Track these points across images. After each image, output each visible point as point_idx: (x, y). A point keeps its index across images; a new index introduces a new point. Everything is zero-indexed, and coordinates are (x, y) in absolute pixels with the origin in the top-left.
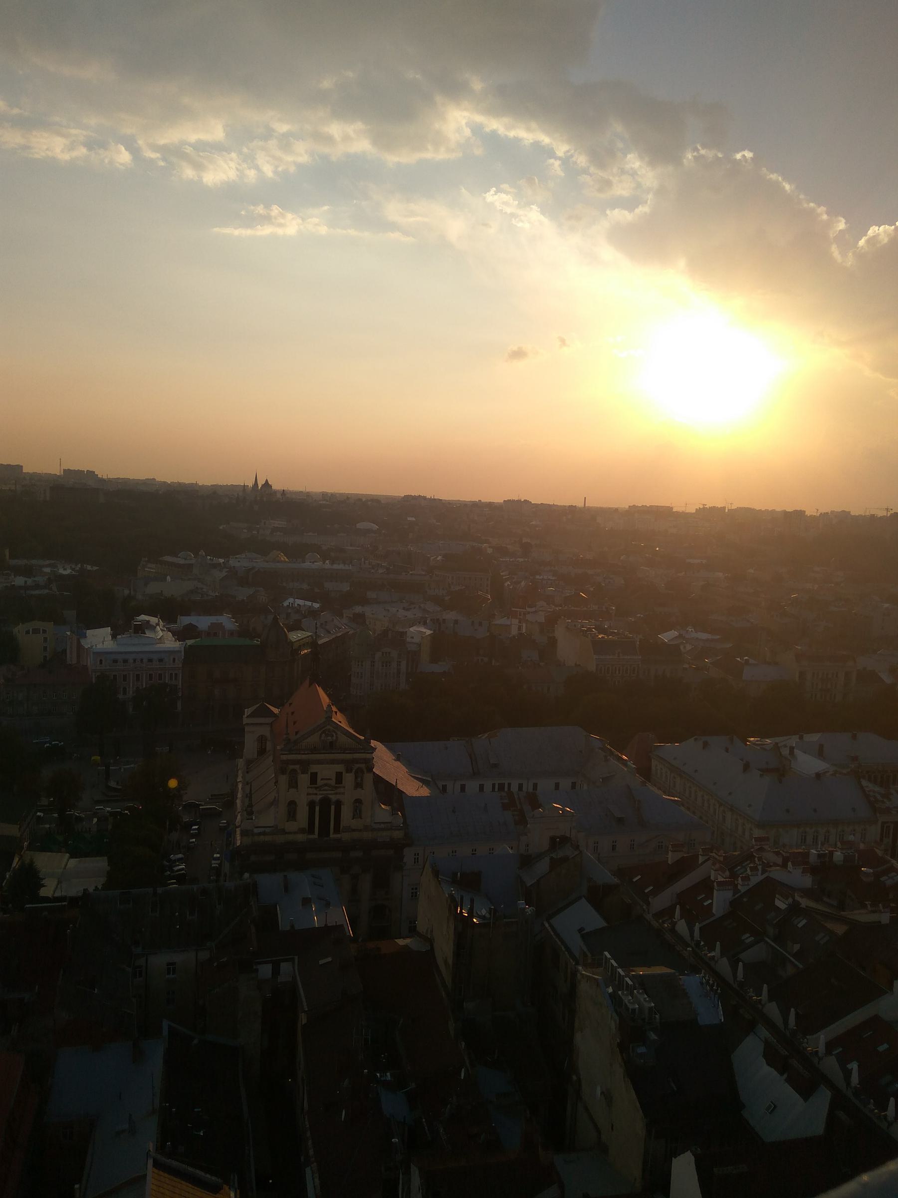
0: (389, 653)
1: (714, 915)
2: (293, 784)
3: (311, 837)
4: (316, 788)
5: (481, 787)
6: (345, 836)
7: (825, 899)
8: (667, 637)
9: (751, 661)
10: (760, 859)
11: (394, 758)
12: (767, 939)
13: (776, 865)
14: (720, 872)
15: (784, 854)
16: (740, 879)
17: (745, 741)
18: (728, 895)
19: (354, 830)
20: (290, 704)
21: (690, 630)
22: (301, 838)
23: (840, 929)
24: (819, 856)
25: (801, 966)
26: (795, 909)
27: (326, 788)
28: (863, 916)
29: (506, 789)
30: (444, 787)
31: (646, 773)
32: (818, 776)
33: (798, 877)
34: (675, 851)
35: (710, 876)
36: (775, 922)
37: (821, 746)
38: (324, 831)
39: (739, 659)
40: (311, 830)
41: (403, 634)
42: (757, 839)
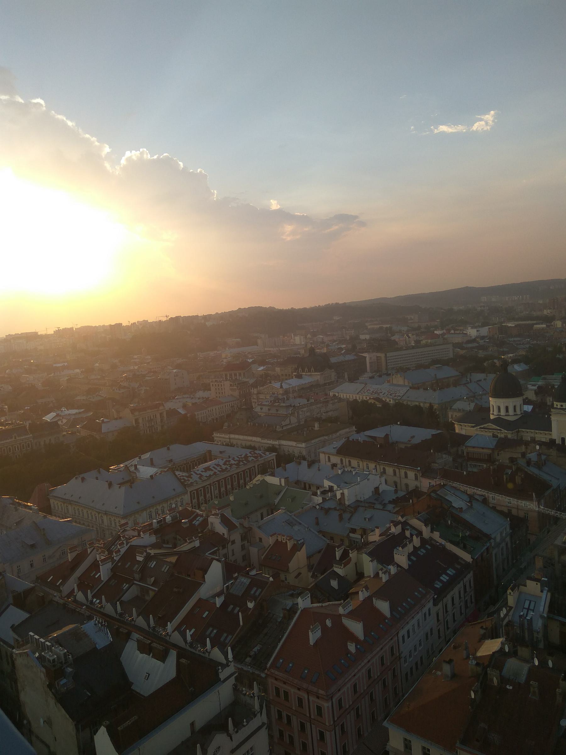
1: (103, 581)
7: (165, 546)
8: (48, 418)
9: (105, 420)
10: (124, 537)
12: (135, 582)
13: (134, 537)
14: (102, 554)
15: (138, 528)
17: (108, 470)
18: (109, 565)
21: (64, 410)
23: (173, 559)
24: (158, 522)
25: (157, 589)
26: (149, 558)
28: (185, 547)
31: (47, 509)
32: (151, 476)
33: (148, 539)
35: (97, 559)
36: (138, 571)
37: (152, 460)
39: (97, 421)
42: (121, 526)
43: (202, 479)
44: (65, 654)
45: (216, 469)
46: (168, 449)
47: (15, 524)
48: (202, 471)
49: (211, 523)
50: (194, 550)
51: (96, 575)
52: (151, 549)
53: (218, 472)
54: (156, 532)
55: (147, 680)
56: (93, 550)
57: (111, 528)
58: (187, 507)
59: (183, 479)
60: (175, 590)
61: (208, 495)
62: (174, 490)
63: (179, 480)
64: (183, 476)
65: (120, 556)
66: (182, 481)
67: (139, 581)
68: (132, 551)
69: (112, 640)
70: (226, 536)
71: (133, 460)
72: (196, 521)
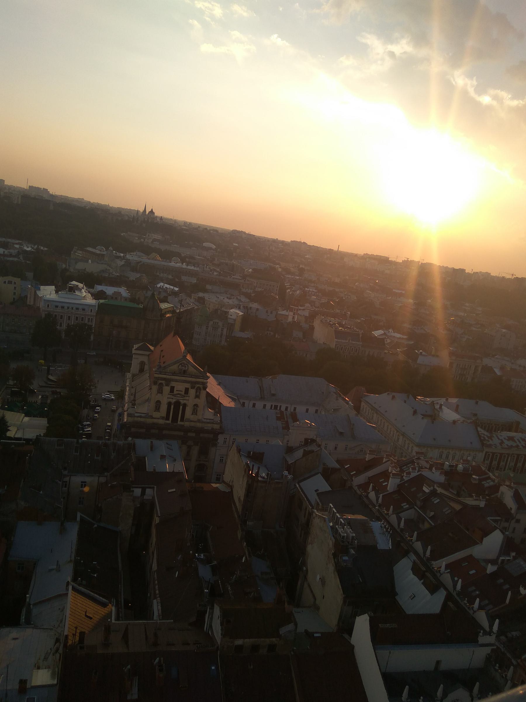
0: (218, 323)
1: (388, 491)
2: (160, 391)
3: (168, 422)
4: (173, 395)
5: (265, 406)
6: (187, 424)
8: (377, 333)
9: (424, 353)
10: (418, 464)
11: (217, 383)
12: (416, 507)
13: (426, 468)
14: (394, 468)
15: (430, 463)
16: (405, 473)
17: (415, 398)
18: (398, 481)
19: (191, 421)
20: (161, 345)
21: (391, 331)
22: (161, 422)
23: (458, 507)
24: (450, 466)
25: (433, 524)
26: (434, 493)
27: (179, 396)
28: (470, 502)
29: (278, 409)
30: (244, 403)
31: (357, 409)
33: (437, 476)
34: (371, 454)
35: (388, 470)
36: (421, 499)
38: (175, 419)
39: (416, 351)
40: (167, 418)
41: (227, 313)
42: (417, 453)
43: (502, 446)
44: (353, 537)
45: (520, 443)
46: (477, 403)
47: (333, 410)
48: (505, 439)
49: (502, 492)
50: (476, 508)
51: (384, 483)
52: (438, 487)
53: (521, 447)
54: (446, 473)
55: (411, 599)
56: (388, 461)
57: (404, 449)
58: (481, 466)
59: (484, 437)
60: (450, 534)
61: (502, 464)
62: (471, 443)
63: (480, 436)
64: (484, 435)
65: (410, 478)
66: (482, 438)
67: (419, 508)
68: (420, 480)
69: (391, 548)
70: (513, 511)
71: (439, 399)
72: (486, 483)
